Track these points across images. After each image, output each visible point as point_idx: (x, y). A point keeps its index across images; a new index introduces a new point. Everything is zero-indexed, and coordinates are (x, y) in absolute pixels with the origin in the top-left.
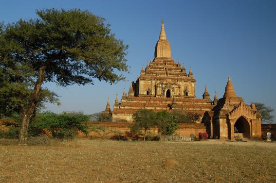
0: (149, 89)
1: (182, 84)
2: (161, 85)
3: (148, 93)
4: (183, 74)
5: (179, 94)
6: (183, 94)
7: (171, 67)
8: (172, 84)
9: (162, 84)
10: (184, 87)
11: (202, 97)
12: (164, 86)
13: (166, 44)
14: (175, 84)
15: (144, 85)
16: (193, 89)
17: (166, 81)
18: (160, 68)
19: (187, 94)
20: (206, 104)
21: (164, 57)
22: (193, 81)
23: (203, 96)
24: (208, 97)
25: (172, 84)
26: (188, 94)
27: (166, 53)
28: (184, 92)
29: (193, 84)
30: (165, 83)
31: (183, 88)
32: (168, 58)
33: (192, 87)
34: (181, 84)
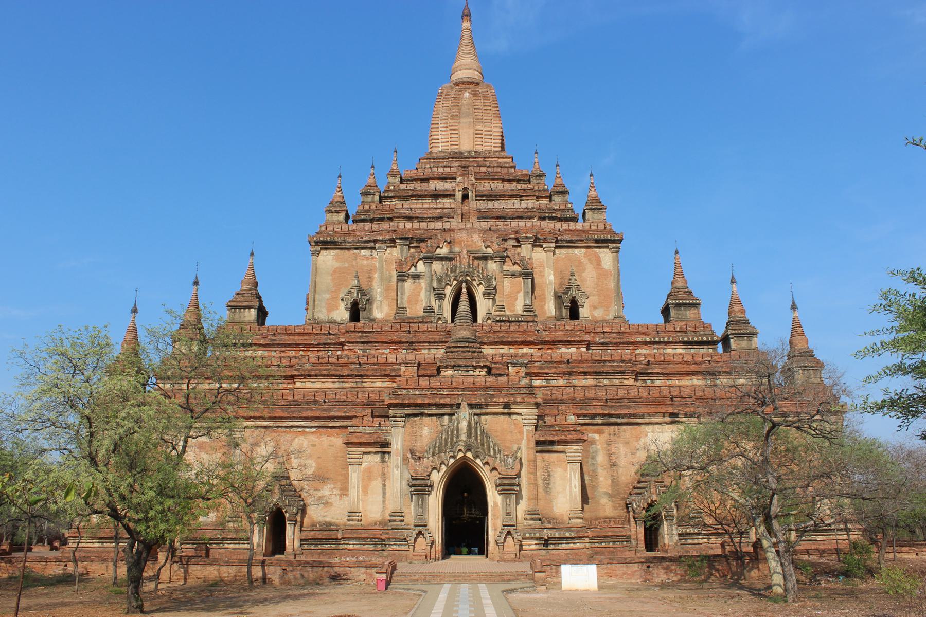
1: (547, 265)
2: (421, 267)
3: (355, 313)
4: (552, 210)
5: (528, 309)
6: (550, 308)
7: (498, 186)
8: (485, 258)
10: (558, 272)
11: (660, 320)
12: (437, 266)
13: (475, 94)
15: (338, 274)
16: (612, 285)
18: (436, 196)
19: (574, 314)
20: (680, 350)
21: (466, 145)
22: (609, 240)
23: (666, 311)
24: (690, 313)
25: (485, 258)
26: (584, 312)
27: (477, 135)
28: (558, 298)
29: (606, 256)
30: (444, 251)
31: (552, 277)
33: (602, 274)
34: (539, 257)
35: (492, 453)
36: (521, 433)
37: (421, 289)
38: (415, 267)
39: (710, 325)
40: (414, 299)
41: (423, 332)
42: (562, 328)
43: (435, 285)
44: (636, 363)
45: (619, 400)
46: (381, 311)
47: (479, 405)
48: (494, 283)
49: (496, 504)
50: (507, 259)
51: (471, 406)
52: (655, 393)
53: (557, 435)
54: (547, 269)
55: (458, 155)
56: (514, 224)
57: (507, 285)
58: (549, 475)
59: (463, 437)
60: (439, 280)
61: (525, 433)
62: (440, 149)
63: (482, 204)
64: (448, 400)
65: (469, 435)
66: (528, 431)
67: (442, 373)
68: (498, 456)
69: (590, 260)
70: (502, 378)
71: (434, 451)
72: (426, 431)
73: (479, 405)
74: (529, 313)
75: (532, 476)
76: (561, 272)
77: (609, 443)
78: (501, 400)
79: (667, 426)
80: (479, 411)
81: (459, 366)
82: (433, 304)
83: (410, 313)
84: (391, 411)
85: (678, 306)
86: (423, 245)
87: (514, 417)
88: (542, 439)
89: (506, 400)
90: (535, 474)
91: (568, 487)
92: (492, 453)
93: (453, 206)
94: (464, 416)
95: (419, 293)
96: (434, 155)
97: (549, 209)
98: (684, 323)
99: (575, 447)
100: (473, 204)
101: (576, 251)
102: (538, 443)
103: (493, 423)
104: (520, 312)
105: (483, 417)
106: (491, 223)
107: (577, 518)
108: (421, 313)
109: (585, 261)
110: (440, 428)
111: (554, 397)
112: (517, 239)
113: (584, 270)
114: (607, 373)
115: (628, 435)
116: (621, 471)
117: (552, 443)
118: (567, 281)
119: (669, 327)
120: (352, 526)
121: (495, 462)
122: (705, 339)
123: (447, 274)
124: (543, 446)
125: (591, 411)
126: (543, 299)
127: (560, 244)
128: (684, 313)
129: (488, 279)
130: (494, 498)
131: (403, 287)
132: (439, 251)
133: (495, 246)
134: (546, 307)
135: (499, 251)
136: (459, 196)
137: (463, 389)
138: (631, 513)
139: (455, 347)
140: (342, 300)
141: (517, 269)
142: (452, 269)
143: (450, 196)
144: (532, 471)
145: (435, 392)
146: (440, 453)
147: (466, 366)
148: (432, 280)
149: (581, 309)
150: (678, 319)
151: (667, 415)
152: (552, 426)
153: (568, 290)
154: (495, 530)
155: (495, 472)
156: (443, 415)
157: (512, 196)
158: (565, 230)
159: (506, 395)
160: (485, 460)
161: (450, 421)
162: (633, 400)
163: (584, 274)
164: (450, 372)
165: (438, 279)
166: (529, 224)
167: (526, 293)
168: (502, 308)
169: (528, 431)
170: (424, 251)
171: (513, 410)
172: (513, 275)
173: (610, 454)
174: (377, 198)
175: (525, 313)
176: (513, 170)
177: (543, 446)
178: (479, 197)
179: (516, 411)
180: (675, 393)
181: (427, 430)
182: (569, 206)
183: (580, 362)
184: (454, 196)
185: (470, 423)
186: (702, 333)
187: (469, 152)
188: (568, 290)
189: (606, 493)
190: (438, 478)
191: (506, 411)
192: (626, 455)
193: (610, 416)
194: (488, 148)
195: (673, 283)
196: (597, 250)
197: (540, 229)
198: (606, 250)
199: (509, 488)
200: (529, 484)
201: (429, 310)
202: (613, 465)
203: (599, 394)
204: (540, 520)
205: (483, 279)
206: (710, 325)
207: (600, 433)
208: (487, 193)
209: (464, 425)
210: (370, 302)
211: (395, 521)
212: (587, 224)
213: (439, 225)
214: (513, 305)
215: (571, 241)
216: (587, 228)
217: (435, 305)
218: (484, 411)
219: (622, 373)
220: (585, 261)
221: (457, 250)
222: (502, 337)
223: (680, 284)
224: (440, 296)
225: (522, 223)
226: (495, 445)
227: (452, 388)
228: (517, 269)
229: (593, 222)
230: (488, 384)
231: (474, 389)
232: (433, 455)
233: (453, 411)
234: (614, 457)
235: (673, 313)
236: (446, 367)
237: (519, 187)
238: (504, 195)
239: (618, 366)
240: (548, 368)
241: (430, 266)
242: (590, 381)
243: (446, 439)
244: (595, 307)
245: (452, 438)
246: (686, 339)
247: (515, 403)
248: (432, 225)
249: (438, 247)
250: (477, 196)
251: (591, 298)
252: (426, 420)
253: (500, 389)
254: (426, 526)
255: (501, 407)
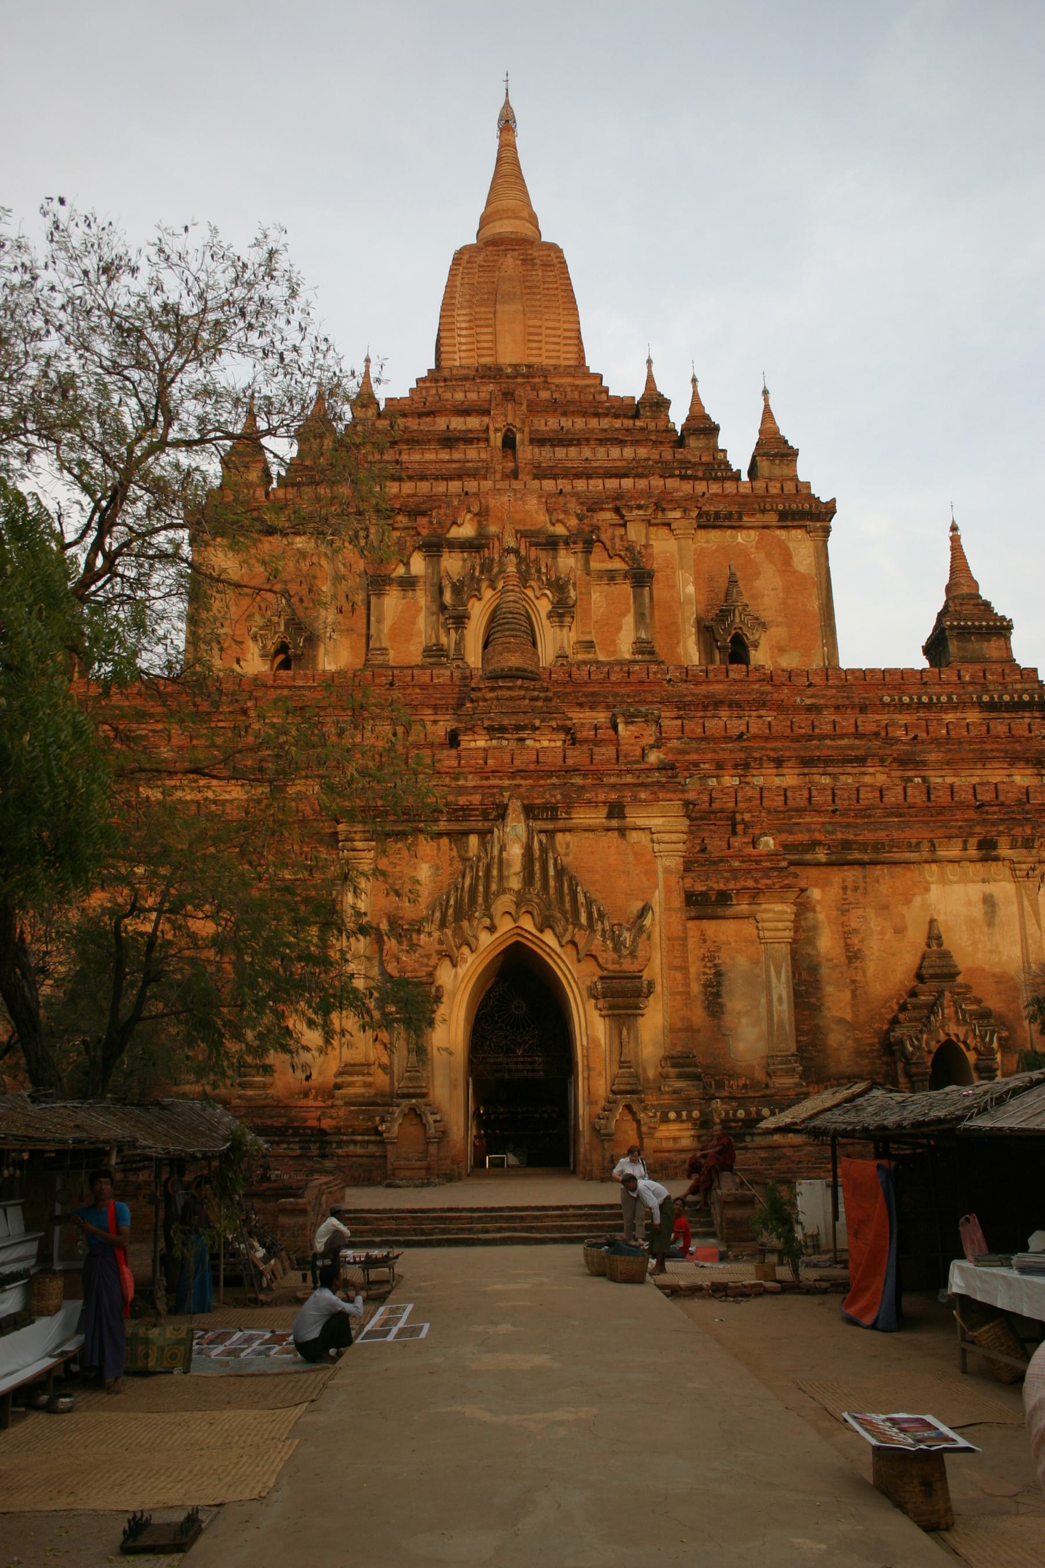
0: (295, 625)
2: (418, 565)
4: (685, 464)
5: (643, 648)
8: (552, 544)
9: (434, 548)
12: (453, 564)
13: (527, 261)
14: (587, 542)
16: (815, 605)
17: (482, 515)
18: (449, 441)
21: (509, 354)
23: (934, 648)
24: (991, 648)
25: (552, 544)
26: (759, 657)
28: (706, 631)
30: (466, 530)
31: (691, 589)
32: (545, 373)
35: (583, 920)
36: (651, 873)
37: (420, 611)
38: (407, 564)
39: (1035, 670)
40: (403, 630)
41: (423, 687)
42: (721, 677)
43: (448, 598)
44: (890, 741)
45: (865, 813)
46: (334, 658)
47: (550, 811)
48: (572, 594)
49: (593, 1041)
50: (597, 549)
51: (530, 811)
52: (942, 797)
53: (735, 879)
54: (680, 573)
55: (492, 373)
56: (612, 484)
57: (598, 597)
58: (719, 974)
59: (515, 883)
60: (457, 590)
61: (661, 875)
62: (457, 364)
63: (546, 455)
64: (476, 799)
65: (528, 879)
66: (667, 870)
67: (464, 745)
68: (599, 926)
69: (769, 556)
70: (603, 750)
71: (444, 915)
72: (424, 872)
73: (550, 811)
74: (647, 657)
75: (679, 975)
76: (711, 579)
77: (844, 908)
78: (602, 797)
79: (971, 868)
80: (550, 826)
81: (502, 729)
82: (444, 640)
83: (393, 658)
84: (341, 827)
85: (964, 633)
86: (423, 521)
87: (634, 836)
88: (700, 887)
89: (614, 796)
90: (684, 969)
91: (763, 1001)
92: (583, 920)
93: (483, 456)
94: (514, 838)
95: (414, 618)
96: (446, 373)
97: (681, 462)
98: (978, 667)
99: (778, 907)
100: (526, 452)
101: (740, 537)
102: (691, 899)
103: (586, 848)
104: (628, 656)
105: (559, 837)
106: (563, 484)
107: (790, 1072)
108: (418, 659)
109: (758, 557)
110: (458, 865)
111: (716, 806)
112: (617, 510)
113: (757, 574)
114: (828, 761)
115: (884, 888)
116: (871, 968)
117: (724, 898)
118: (722, 596)
119: (948, 675)
120: (250, 1099)
121: (590, 941)
122: (1026, 697)
123: (473, 575)
124: (703, 905)
125: (803, 837)
126: (674, 635)
127: (708, 522)
128: (977, 646)
129: (559, 586)
130: (590, 1025)
131: (381, 606)
132: (455, 532)
133: (573, 522)
134: (680, 650)
135: (580, 531)
136: (497, 439)
137: (513, 775)
138: (900, 1066)
139: (493, 689)
140: (255, 638)
141: (618, 565)
142: (482, 566)
143: (478, 440)
144: (677, 962)
145: (447, 781)
146: (458, 917)
147: (519, 728)
148: (441, 592)
149: (752, 653)
150: (964, 660)
151: (973, 842)
152: (722, 860)
153: (724, 614)
154: (591, 1102)
155: (589, 966)
156: (466, 833)
157: (601, 442)
158: (717, 495)
159: (613, 786)
160: (568, 937)
161: (483, 844)
162: (896, 811)
163: (757, 584)
164: (481, 744)
165: (453, 585)
166: (642, 483)
167: (640, 618)
168: (589, 645)
169: (667, 870)
170: (425, 532)
171: (630, 821)
172: (611, 576)
173: (847, 934)
174: (328, 443)
175: (639, 657)
176: (603, 397)
177: (703, 905)
178: (538, 441)
179: (640, 822)
180: (987, 797)
181: (427, 867)
182: (720, 456)
183: (767, 739)
184: (487, 440)
185: (528, 849)
186: (1019, 686)
187: (515, 366)
188: (724, 614)
189: (841, 1021)
190: (458, 983)
191: (614, 823)
192: (882, 933)
193: (846, 845)
194: (553, 362)
195: (948, 589)
196: (782, 534)
197: (665, 492)
198: (799, 533)
199: (623, 997)
200: (673, 994)
201: (435, 653)
202: (853, 956)
203: (817, 799)
204: (697, 1077)
205: (550, 585)
206: (1035, 670)
207: (824, 885)
208: (552, 435)
209: (515, 851)
210: (312, 641)
211: (351, 1084)
212: (760, 485)
213: (455, 486)
214: (614, 642)
215: (729, 516)
216: (761, 492)
217: (448, 640)
218: (561, 824)
219: (861, 760)
220: (758, 557)
221: (493, 529)
222: (593, 694)
223: (965, 590)
224: (460, 621)
225: (627, 483)
226: (589, 902)
227: (483, 773)
228: (618, 565)
229: (770, 479)
230: (570, 762)
231: (538, 771)
232: (443, 924)
233: (487, 825)
234: (855, 940)
235: (953, 647)
236: (471, 730)
237: (617, 423)
238: (588, 440)
239: (851, 748)
240: (697, 751)
241: (439, 563)
242: (790, 779)
243: (473, 889)
244: (781, 650)
245: (487, 887)
246: (986, 698)
247: (635, 799)
248: (440, 487)
249: (455, 523)
250: (532, 441)
251: (773, 631)
252: (426, 847)
253: (598, 775)
254: (424, 1095)
255: (603, 812)
